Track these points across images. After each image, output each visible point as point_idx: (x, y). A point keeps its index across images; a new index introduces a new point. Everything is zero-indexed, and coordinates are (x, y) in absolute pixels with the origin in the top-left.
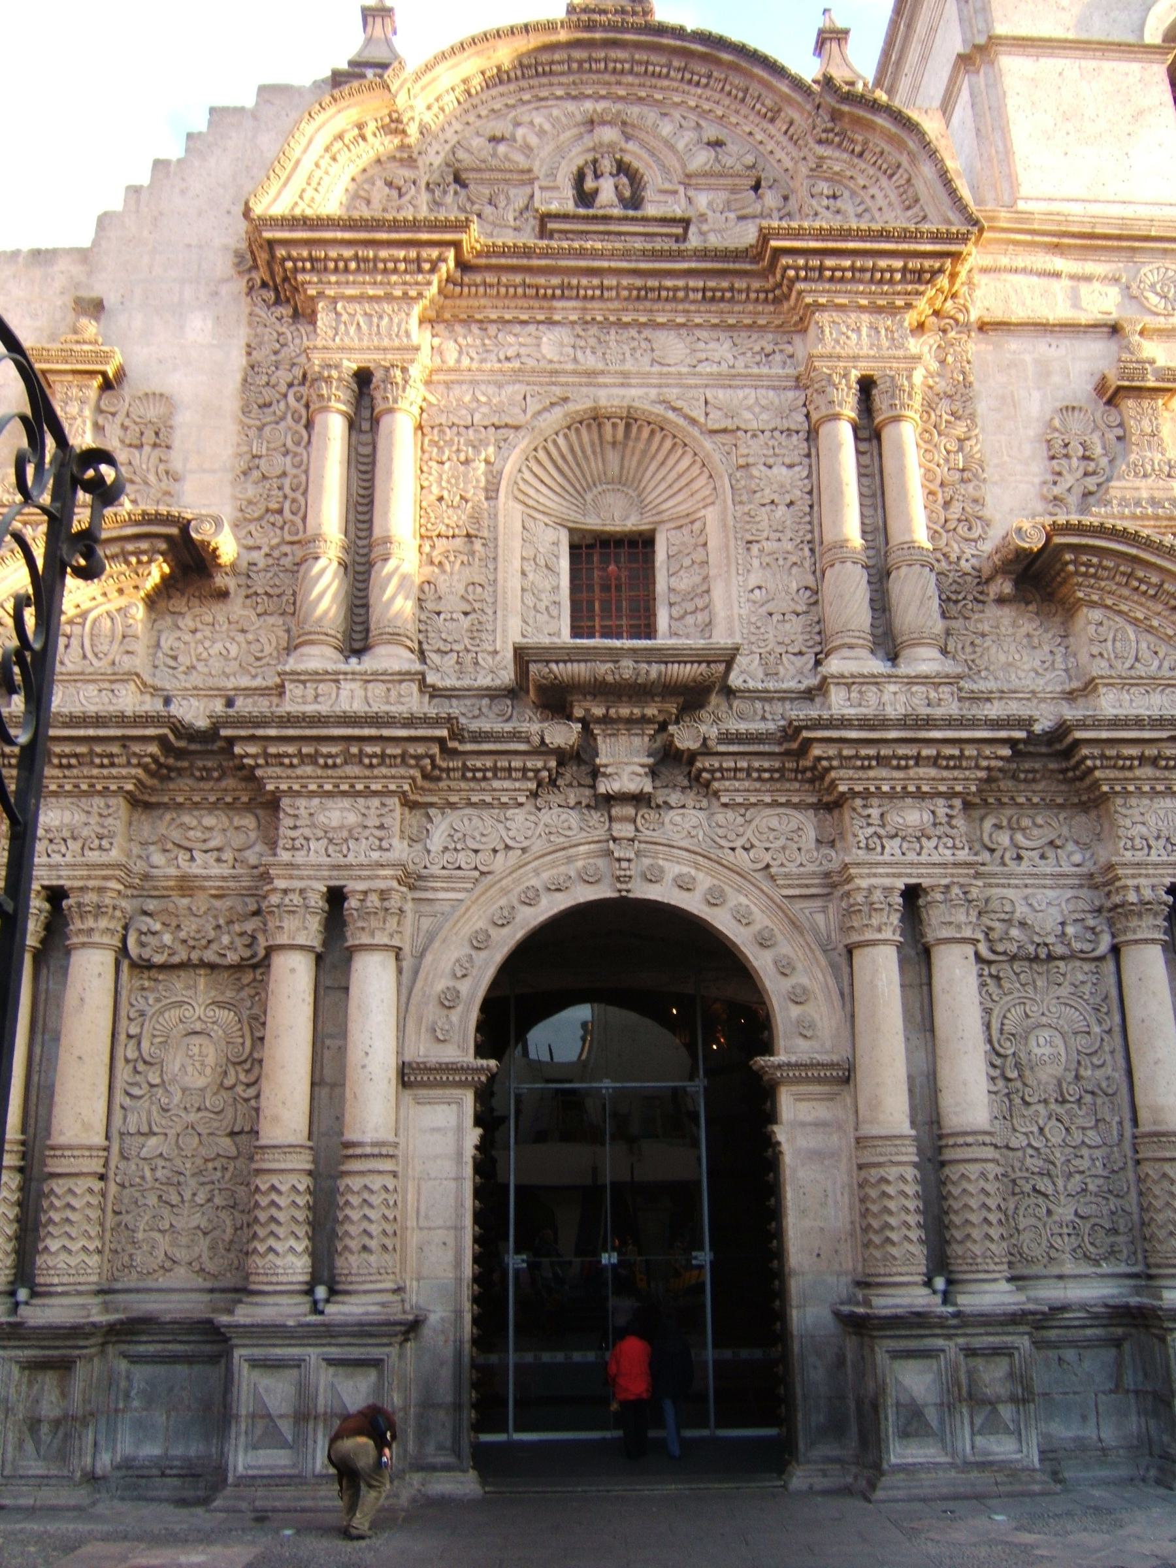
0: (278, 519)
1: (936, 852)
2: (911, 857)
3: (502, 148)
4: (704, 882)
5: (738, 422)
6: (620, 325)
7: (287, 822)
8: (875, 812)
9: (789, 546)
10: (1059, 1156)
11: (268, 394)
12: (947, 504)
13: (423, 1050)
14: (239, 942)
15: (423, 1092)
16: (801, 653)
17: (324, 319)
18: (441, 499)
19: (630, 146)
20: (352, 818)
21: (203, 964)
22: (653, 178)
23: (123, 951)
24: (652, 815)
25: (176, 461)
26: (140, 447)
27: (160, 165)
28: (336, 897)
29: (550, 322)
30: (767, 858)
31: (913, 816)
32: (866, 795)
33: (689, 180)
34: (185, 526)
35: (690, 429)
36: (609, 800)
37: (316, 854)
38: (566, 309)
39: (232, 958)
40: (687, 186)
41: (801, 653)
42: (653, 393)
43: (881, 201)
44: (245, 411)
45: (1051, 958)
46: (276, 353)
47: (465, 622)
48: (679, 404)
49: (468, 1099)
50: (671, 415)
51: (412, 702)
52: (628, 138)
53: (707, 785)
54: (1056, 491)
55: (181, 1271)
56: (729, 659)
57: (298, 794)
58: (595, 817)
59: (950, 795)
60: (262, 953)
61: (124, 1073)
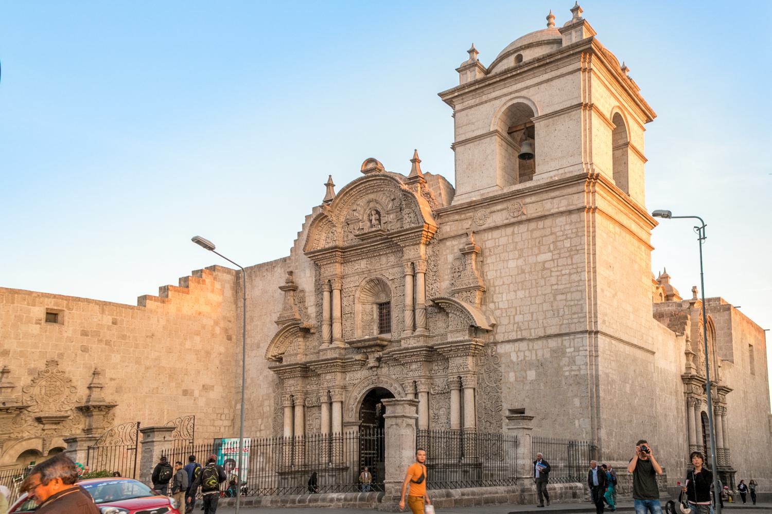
1: (417, 374)
3: (355, 213)
6: (374, 256)
13: (346, 419)
15: (348, 427)
17: (322, 270)
20: (330, 377)
21: (316, 406)
23: (304, 406)
24: (379, 369)
27: (299, 233)
29: (362, 259)
31: (414, 366)
32: (406, 363)
36: (371, 368)
37: (325, 385)
38: (364, 256)
40: (387, 214)
44: (315, 291)
45: (444, 393)
47: (351, 332)
54: (452, 282)
57: (323, 373)
58: (371, 371)
59: (420, 361)
61: (307, 427)
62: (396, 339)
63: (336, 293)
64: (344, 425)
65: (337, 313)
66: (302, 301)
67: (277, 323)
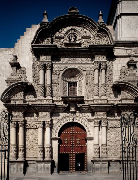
0: (37, 82)
2: (101, 118)
4: (80, 120)
5: (86, 69)
7: (39, 114)
8: (97, 113)
9: (91, 84)
10: (113, 146)
11: (35, 67)
12: (108, 79)
13: (54, 136)
14: (36, 126)
16: (91, 96)
18: (54, 79)
19: (75, 33)
20: (46, 114)
22: (78, 38)
25: (26, 75)
26: (22, 73)
28: (44, 122)
30: (87, 118)
33: (83, 38)
34: (27, 83)
35: (81, 70)
39: (35, 128)
41: (91, 96)
42: (77, 66)
43: (104, 40)
46: (36, 62)
48: (80, 67)
49: (57, 141)
50: (78, 68)
51: (50, 102)
52: (75, 31)
53: (81, 110)
54: (121, 77)
55: (32, 156)
56: (83, 97)
60: (38, 127)
62: (86, 100)
63: (48, 72)
64: (52, 139)
65: (48, 82)
66: (24, 73)
67: (7, 82)
